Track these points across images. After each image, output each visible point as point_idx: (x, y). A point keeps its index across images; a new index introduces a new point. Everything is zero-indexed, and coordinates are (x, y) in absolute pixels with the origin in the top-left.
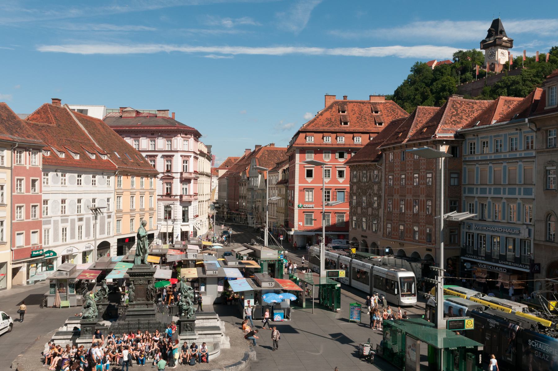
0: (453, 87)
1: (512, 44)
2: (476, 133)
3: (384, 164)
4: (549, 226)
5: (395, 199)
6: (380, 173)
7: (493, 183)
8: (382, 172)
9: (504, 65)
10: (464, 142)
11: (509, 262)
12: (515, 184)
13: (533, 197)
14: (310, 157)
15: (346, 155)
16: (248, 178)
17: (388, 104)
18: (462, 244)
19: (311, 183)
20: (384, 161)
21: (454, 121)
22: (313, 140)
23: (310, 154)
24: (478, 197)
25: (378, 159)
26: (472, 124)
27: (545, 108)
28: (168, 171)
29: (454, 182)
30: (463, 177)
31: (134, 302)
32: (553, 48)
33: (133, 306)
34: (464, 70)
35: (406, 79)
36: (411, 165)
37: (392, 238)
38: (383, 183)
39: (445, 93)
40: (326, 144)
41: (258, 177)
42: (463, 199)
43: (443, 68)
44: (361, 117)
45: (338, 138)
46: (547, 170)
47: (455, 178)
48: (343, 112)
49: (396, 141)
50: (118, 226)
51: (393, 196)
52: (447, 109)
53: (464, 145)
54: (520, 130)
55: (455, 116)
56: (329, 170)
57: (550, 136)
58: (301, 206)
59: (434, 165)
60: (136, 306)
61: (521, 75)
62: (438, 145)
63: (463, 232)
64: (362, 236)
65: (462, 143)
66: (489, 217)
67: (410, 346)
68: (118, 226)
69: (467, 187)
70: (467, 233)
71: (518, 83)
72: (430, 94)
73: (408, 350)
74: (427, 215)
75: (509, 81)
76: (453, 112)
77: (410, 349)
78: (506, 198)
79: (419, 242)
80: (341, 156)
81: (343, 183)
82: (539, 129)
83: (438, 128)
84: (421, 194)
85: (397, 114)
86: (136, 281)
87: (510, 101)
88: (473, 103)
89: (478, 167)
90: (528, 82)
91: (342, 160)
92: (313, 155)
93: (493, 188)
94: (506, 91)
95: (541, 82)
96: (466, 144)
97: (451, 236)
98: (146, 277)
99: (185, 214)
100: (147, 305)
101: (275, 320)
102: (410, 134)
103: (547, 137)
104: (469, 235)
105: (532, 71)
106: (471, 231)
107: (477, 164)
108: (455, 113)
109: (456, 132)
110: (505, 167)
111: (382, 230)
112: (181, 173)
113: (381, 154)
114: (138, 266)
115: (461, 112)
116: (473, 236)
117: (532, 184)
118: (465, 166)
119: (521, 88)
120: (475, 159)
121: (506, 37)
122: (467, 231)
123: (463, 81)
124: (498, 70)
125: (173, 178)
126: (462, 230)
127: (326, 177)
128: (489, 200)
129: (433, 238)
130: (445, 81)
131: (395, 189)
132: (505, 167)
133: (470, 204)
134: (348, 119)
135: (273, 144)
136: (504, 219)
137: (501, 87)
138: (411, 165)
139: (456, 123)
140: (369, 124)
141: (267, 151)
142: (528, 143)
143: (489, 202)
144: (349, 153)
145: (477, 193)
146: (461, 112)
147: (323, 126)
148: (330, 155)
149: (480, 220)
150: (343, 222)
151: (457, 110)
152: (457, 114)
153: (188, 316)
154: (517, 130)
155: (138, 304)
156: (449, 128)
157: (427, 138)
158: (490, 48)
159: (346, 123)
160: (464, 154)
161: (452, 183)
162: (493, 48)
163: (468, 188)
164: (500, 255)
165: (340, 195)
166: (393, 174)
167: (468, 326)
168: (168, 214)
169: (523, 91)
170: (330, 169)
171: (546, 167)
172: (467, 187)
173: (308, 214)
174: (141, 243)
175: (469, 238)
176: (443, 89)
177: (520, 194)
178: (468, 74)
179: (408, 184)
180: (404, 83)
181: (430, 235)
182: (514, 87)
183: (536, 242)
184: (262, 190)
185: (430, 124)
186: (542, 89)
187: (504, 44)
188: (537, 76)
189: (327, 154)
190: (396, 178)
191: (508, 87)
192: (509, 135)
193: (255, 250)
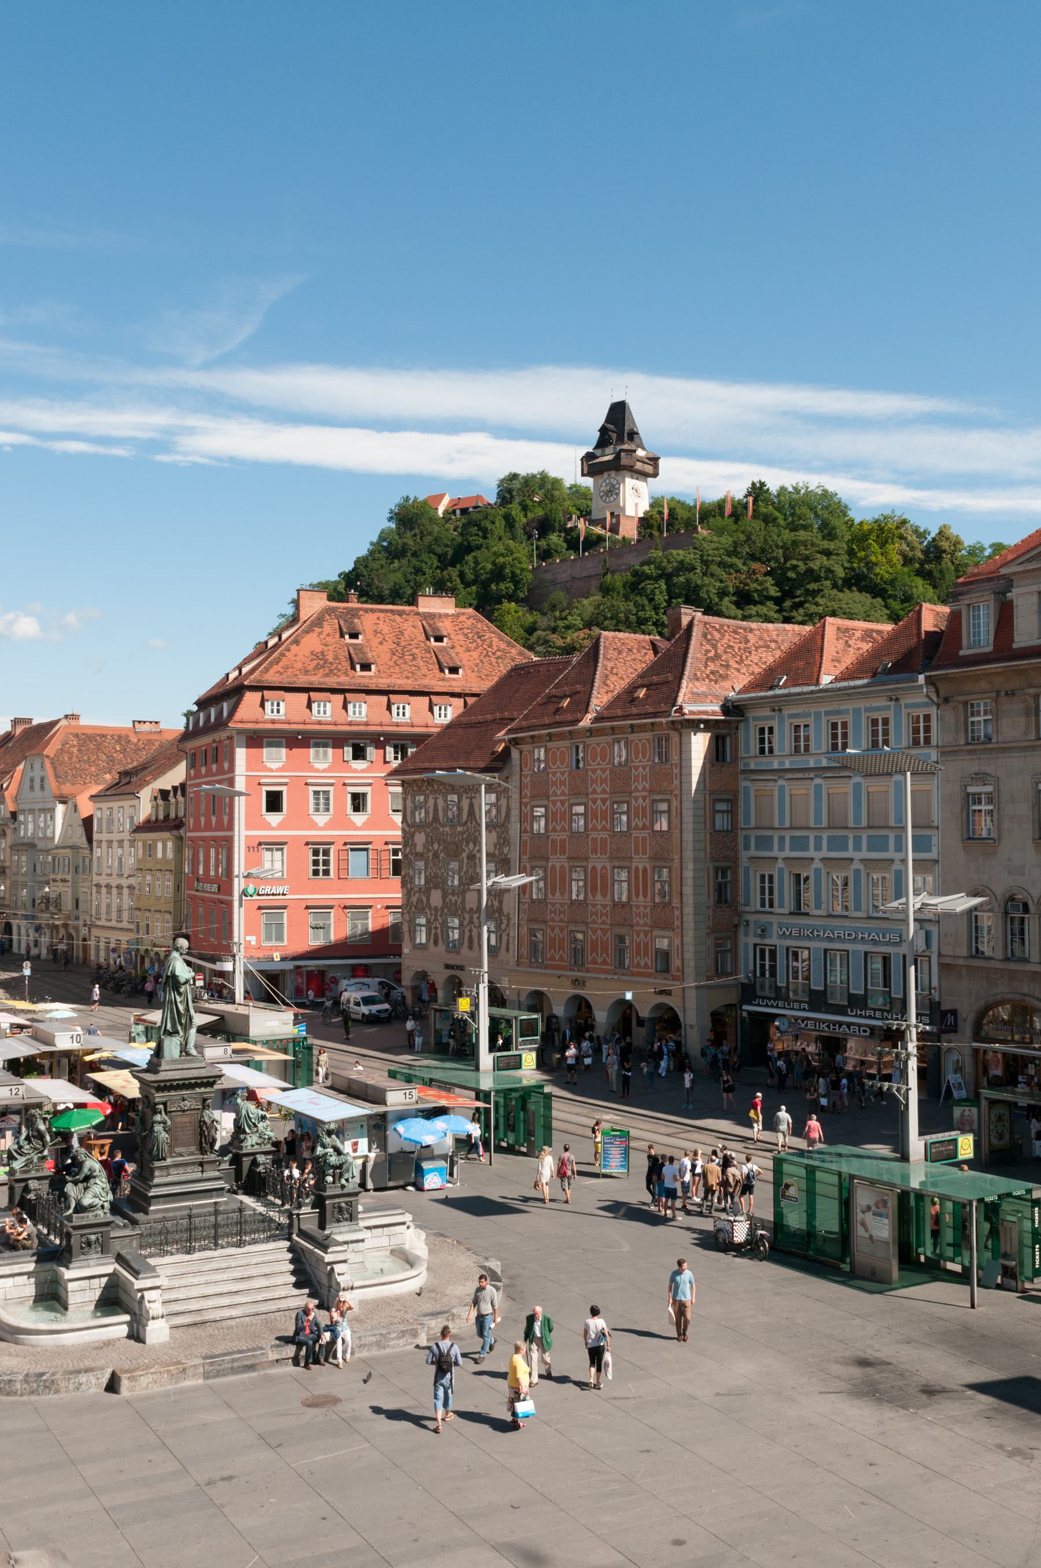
0: (522, 570)
1: (656, 467)
2: (777, 705)
3: (516, 778)
4: (976, 922)
5: (553, 867)
6: (503, 802)
7: (825, 824)
8: (509, 798)
9: (641, 520)
10: (742, 726)
11: (875, 1010)
12: (887, 827)
13: (933, 855)
14: (275, 760)
15: (371, 752)
16: (14, 815)
17: (462, 618)
20: (517, 769)
21: (712, 672)
22: (329, 713)
23: (274, 750)
24: (786, 859)
25: (498, 764)
26: (766, 680)
27: (962, 653)
29: (721, 822)
30: (741, 811)
31: (169, 1161)
32: (753, 484)
33: (164, 1172)
34: (545, 526)
35: (375, 539)
36: (603, 781)
37: (546, 968)
38: (514, 828)
39: (502, 586)
40: (319, 723)
41: (52, 810)
42: (744, 862)
43: (486, 518)
44: (400, 652)
45: (350, 707)
46: (968, 794)
47: (722, 812)
48: (354, 636)
49: (558, 718)
51: (547, 859)
52: (693, 642)
53: (741, 733)
54: (897, 700)
55: (713, 659)
56: (326, 793)
57: (973, 715)
58: (251, 890)
59: (676, 782)
60: (172, 1171)
61: (695, 548)
62: (684, 731)
63: (746, 945)
64: (448, 967)
65: (737, 729)
66: (818, 906)
67: (869, 1208)
69: (753, 834)
70: (755, 945)
71: (693, 569)
72: (460, 586)
73: (860, 1216)
74: (655, 906)
75: (669, 562)
76: (707, 651)
77: (869, 1216)
78: (862, 861)
79: (633, 974)
80: (359, 754)
81: (384, 825)
82: (946, 700)
83: (683, 691)
84: (637, 852)
85: (490, 646)
86: (173, 1102)
87: (847, 630)
88: (745, 630)
89: (782, 789)
90: (714, 568)
91: (359, 765)
92: (284, 750)
93: (825, 836)
94: (664, 587)
95: (745, 568)
96: (747, 729)
97: (717, 953)
98: (198, 1090)
100: (201, 1164)
101: (427, 1186)
102: (599, 700)
103: (966, 718)
104: (763, 952)
105: (723, 540)
106: (767, 941)
107: (816, 776)
108: (712, 654)
109: (726, 700)
110: (857, 787)
111: (513, 948)
113: (507, 751)
114: (174, 1061)
115: (725, 652)
116: (773, 954)
117: (931, 827)
118: (747, 783)
119: (699, 582)
120: (776, 766)
121: (644, 449)
122: (758, 941)
123: (545, 555)
124: (629, 530)
126: (742, 939)
127: (317, 810)
128: (817, 864)
129: (676, 962)
130: (502, 555)
131: (554, 842)
132: (857, 787)
133: (763, 877)
134: (370, 655)
135: (74, 717)
136: (858, 908)
137: (649, 577)
138: (603, 781)
139: (718, 677)
140: (424, 671)
141: (77, 736)
142: (916, 731)
143: (817, 871)
144: (380, 745)
145: (781, 848)
146: (725, 652)
148: (330, 750)
149: (791, 914)
150: (366, 932)
151: (715, 647)
152: (717, 657)
153: (343, 1181)
154: (891, 700)
155: (177, 1166)
156: (704, 689)
157: (655, 715)
158: (606, 475)
160: (742, 754)
161: (718, 826)
162: (613, 473)
163: (757, 837)
164: (850, 995)
165: (358, 860)
166: (545, 802)
167: (963, 1152)
169: (705, 589)
170: (331, 789)
171: (966, 787)
172: (753, 834)
173: (272, 909)
174: (178, 999)
175: (763, 958)
176: (498, 574)
177: (818, 848)
178: (555, 539)
179: (594, 829)
180: (371, 553)
181: (665, 956)
182: (682, 579)
183: (946, 961)
184: (72, 847)
185: (655, 679)
186: (946, 610)
187: (639, 466)
188: (733, 552)
189: (321, 750)
190: (554, 814)
191: (668, 577)
192: (867, 710)
193: (222, 1017)
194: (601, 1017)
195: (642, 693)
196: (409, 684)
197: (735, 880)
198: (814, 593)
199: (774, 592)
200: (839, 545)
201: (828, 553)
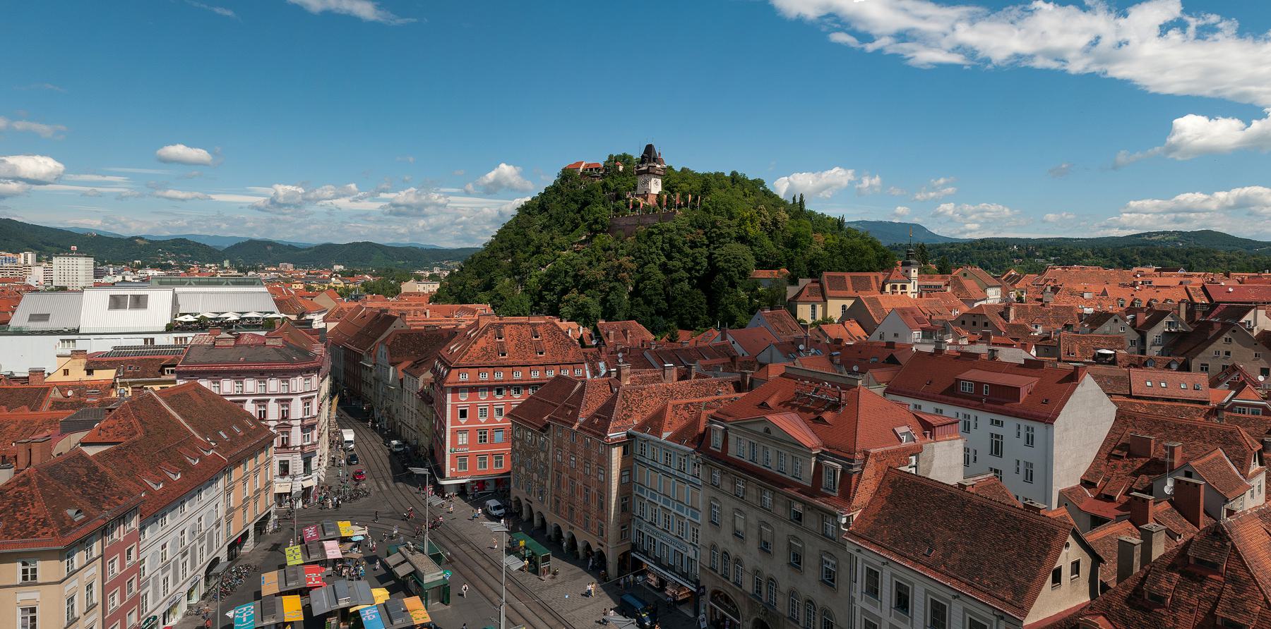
14: (464, 398)
15: (504, 392)
18: (633, 540)
28: (284, 418)
50: (228, 529)
68: (228, 529)
80: (499, 392)
91: (499, 397)
99: (307, 464)
102: (581, 419)
112: (303, 420)
124: (652, 201)
125: (292, 426)
144: (508, 389)
159: (504, 355)
168: (285, 469)
173: (461, 460)
176: (596, 221)
194: (579, 544)
195: (596, 421)
196: (521, 362)
198: (723, 243)
199: (706, 242)
200: (735, 222)
201: (729, 226)
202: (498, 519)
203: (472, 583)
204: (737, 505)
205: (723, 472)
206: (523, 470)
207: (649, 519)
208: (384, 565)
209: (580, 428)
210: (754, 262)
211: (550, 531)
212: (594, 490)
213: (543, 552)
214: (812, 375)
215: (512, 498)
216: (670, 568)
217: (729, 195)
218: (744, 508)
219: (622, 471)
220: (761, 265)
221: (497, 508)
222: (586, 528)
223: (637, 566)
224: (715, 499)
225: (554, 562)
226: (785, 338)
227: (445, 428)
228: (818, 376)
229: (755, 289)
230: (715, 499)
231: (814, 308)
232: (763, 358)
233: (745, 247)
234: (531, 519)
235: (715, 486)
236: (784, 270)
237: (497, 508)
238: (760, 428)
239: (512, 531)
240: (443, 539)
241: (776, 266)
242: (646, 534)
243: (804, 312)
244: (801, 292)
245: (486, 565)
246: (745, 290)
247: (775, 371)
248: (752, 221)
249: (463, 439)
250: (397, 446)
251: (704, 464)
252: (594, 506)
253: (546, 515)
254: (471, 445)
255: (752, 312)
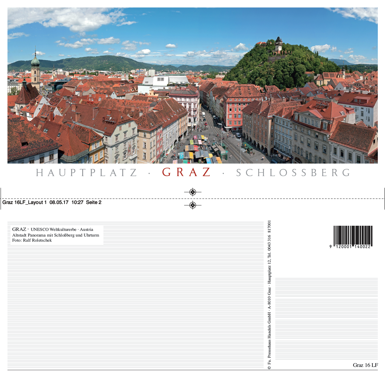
14: (231, 105)
15: (241, 104)
18: (274, 145)
19: (231, 112)
80: (240, 104)
102: (261, 112)
135: (212, 82)
144: (242, 104)
147: (234, 95)
173: (230, 122)
196: (245, 96)
197: (274, 134)
202: (239, 138)
203: (233, 155)
204: (301, 134)
205: (298, 126)
206: (246, 125)
207: (278, 139)
208: (212, 148)
209: (260, 114)
210: (306, 69)
211: (253, 142)
212: (264, 131)
213: (251, 147)
214: (320, 99)
215: (243, 133)
216: (284, 152)
217: (299, 51)
218: (303, 135)
219: (271, 126)
220: (308, 70)
221: (239, 135)
222: (262, 141)
223: (276, 152)
224: (296, 133)
225: (254, 151)
226: (314, 90)
227: (226, 113)
228: (322, 100)
229: (306, 77)
230: (296, 133)
231: (321, 82)
232: (308, 95)
233: (303, 65)
234: (248, 139)
235: (296, 130)
236: (313, 72)
237: (239, 135)
238: (307, 114)
239: (243, 141)
240: (225, 142)
241: (311, 71)
242: (278, 143)
243: (318, 83)
244: (317, 78)
245: (236, 150)
246: (304, 77)
247: (311, 99)
248: (305, 58)
249: (231, 116)
250: (215, 117)
251: (293, 124)
252: (264, 136)
253: (251, 138)
254: (232, 118)
255: (305, 83)
